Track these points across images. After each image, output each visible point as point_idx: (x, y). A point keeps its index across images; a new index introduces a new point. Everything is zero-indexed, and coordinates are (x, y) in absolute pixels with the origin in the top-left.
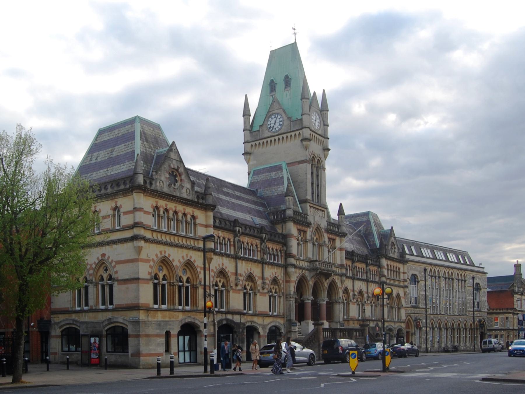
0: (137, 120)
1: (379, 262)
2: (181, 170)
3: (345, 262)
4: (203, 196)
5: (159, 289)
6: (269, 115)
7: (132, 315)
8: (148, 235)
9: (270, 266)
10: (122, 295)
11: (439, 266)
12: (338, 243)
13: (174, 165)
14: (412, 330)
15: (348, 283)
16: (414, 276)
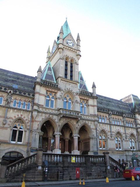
1: (135, 117)
9: (16, 110)
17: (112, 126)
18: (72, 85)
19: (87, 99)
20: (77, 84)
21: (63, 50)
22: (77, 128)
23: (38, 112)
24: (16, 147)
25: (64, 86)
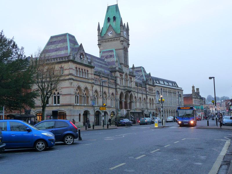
0: (67, 35)
2: (84, 54)
3: (135, 86)
4: (90, 63)
5: (77, 97)
6: (108, 30)
7: (69, 107)
8: (74, 78)
10: (63, 100)
11: (166, 87)
12: (133, 79)
13: (82, 52)
14: (158, 113)
15: (136, 95)
16: (158, 91)
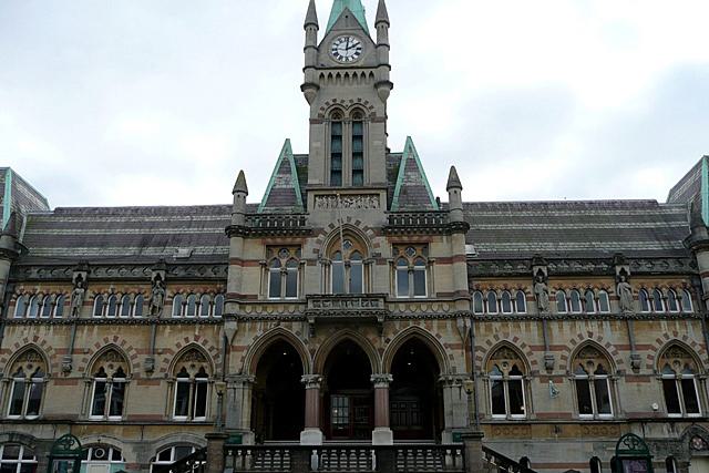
17: (554, 326)
18: (359, 203)
19: (425, 238)
20: (378, 195)
21: (318, 88)
22: (381, 350)
23: (240, 320)
24: (185, 431)
25: (328, 214)
